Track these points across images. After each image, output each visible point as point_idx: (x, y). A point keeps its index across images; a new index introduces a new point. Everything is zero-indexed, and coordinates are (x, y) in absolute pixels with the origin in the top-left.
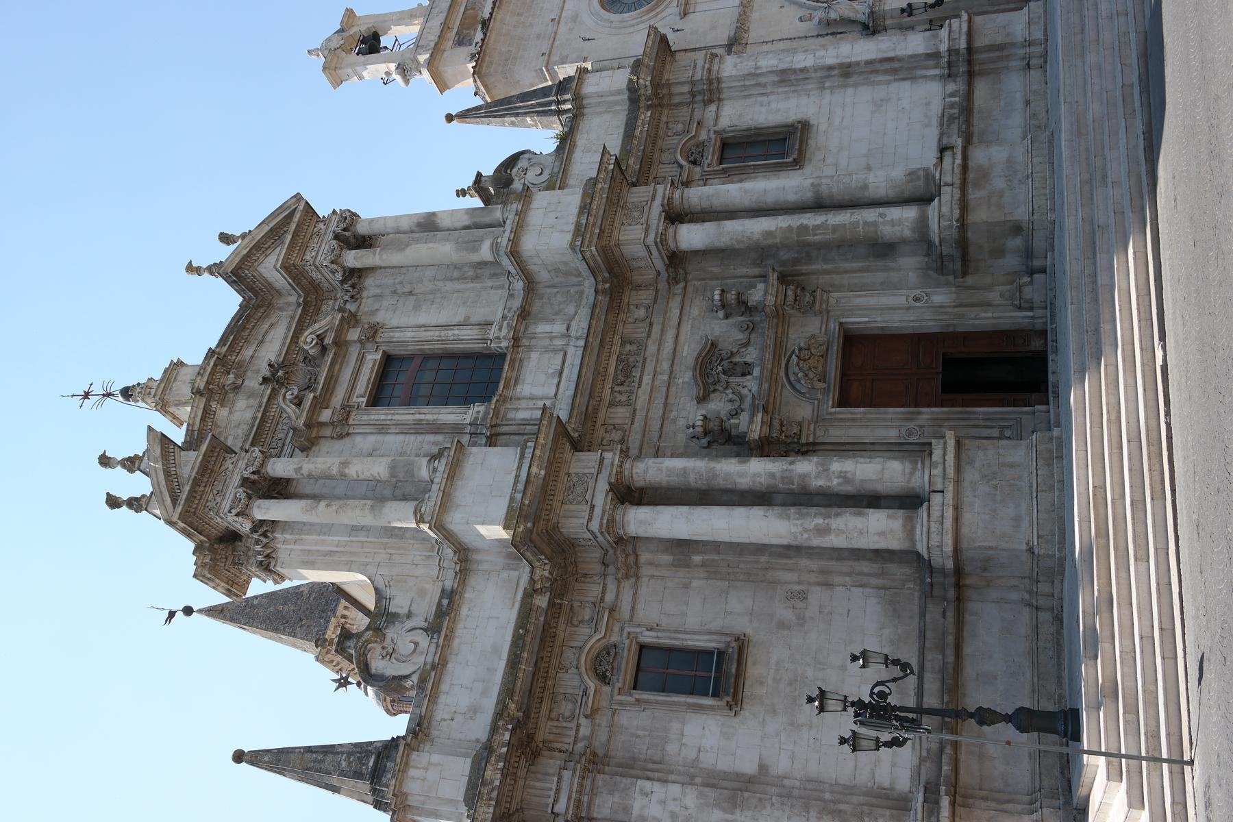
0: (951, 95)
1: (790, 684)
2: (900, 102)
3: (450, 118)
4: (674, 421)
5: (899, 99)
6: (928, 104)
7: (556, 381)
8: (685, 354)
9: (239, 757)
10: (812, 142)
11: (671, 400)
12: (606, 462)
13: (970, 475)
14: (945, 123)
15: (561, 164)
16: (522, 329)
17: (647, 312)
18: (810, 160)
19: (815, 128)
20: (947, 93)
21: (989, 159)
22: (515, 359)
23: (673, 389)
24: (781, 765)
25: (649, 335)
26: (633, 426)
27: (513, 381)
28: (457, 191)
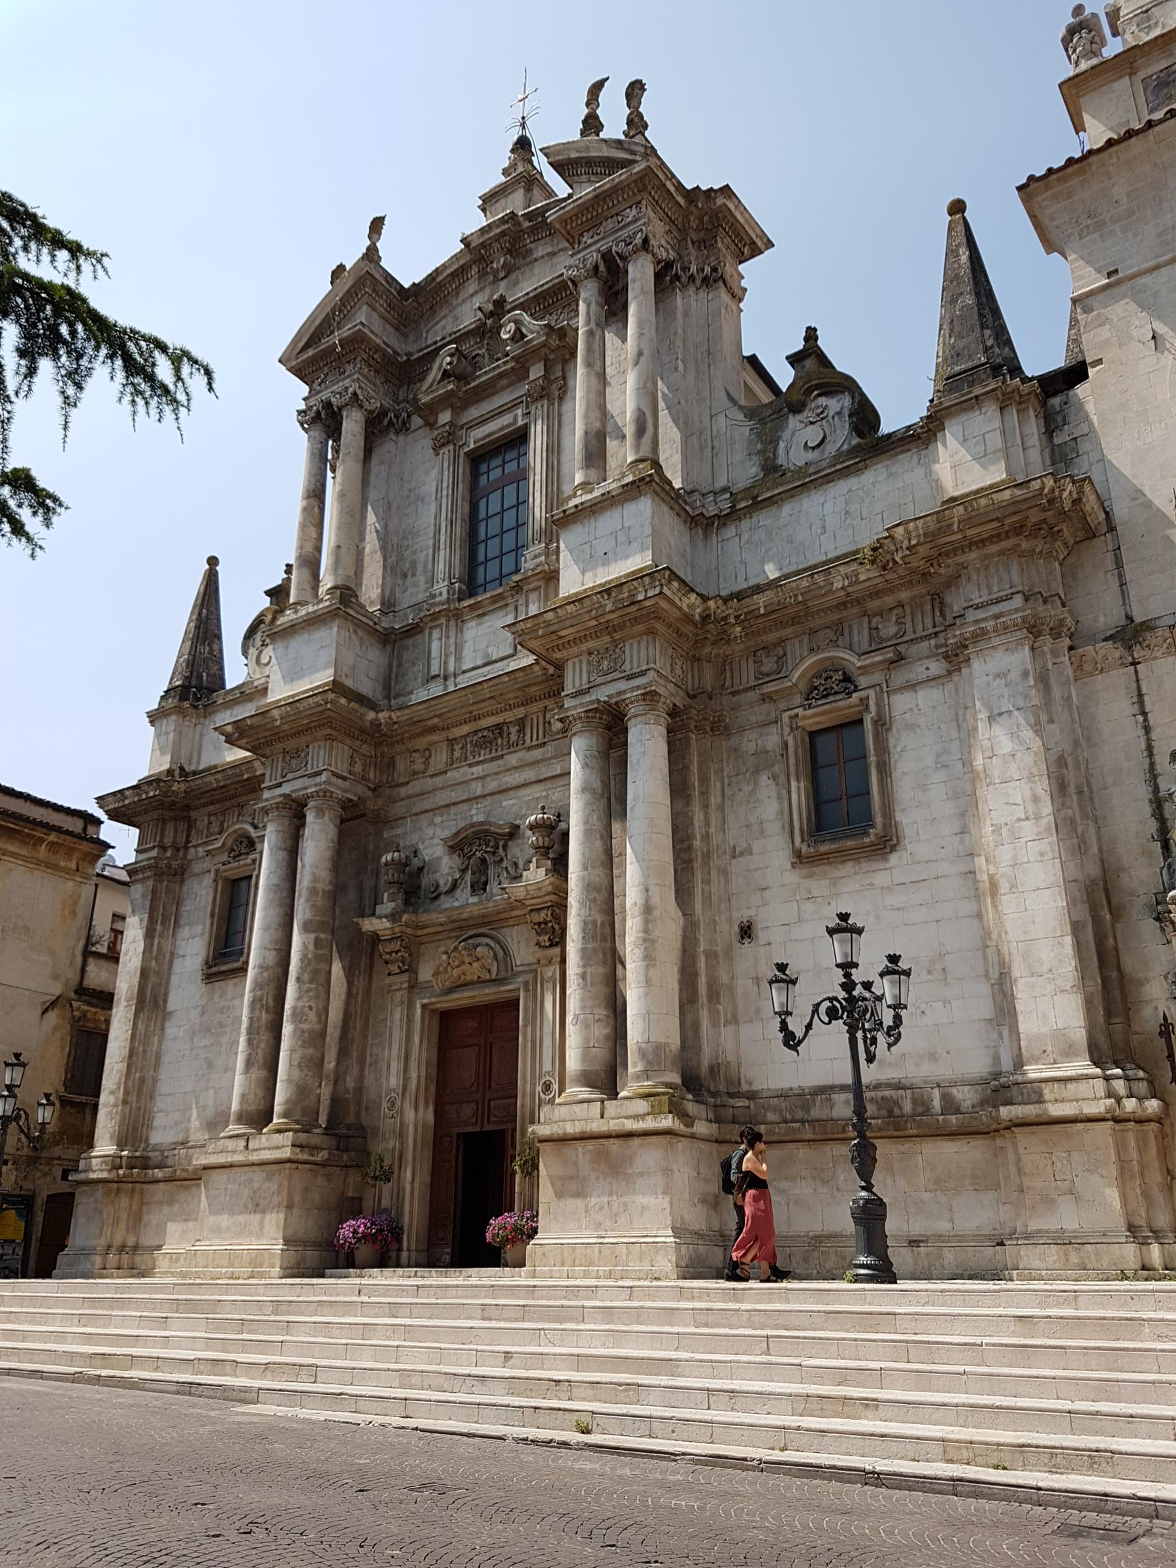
0: (947, 1099)
1: (219, 1023)
2: (940, 1004)
3: (957, 207)
4: (431, 824)
5: (946, 1002)
6: (933, 1057)
7: (479, 663)
8: (504, 804)
9: (213, 561)
10: (849, 867)
11: (453, 810)
12: (318, 779)
13: (258, 1176)
14: (880, 1094)
15: (830, 467)
16: (532, 586)
17: (556, 734)
18: (810, 876)
19: (880, 865)
20: (954, 1091)
21: (642, 1174)
22: (504, 598)
23: (465, 807)
24: (171, 1030)
25: (529, 749)
26: (428, 779)
27: (480, 611)
28: (815, 330)
